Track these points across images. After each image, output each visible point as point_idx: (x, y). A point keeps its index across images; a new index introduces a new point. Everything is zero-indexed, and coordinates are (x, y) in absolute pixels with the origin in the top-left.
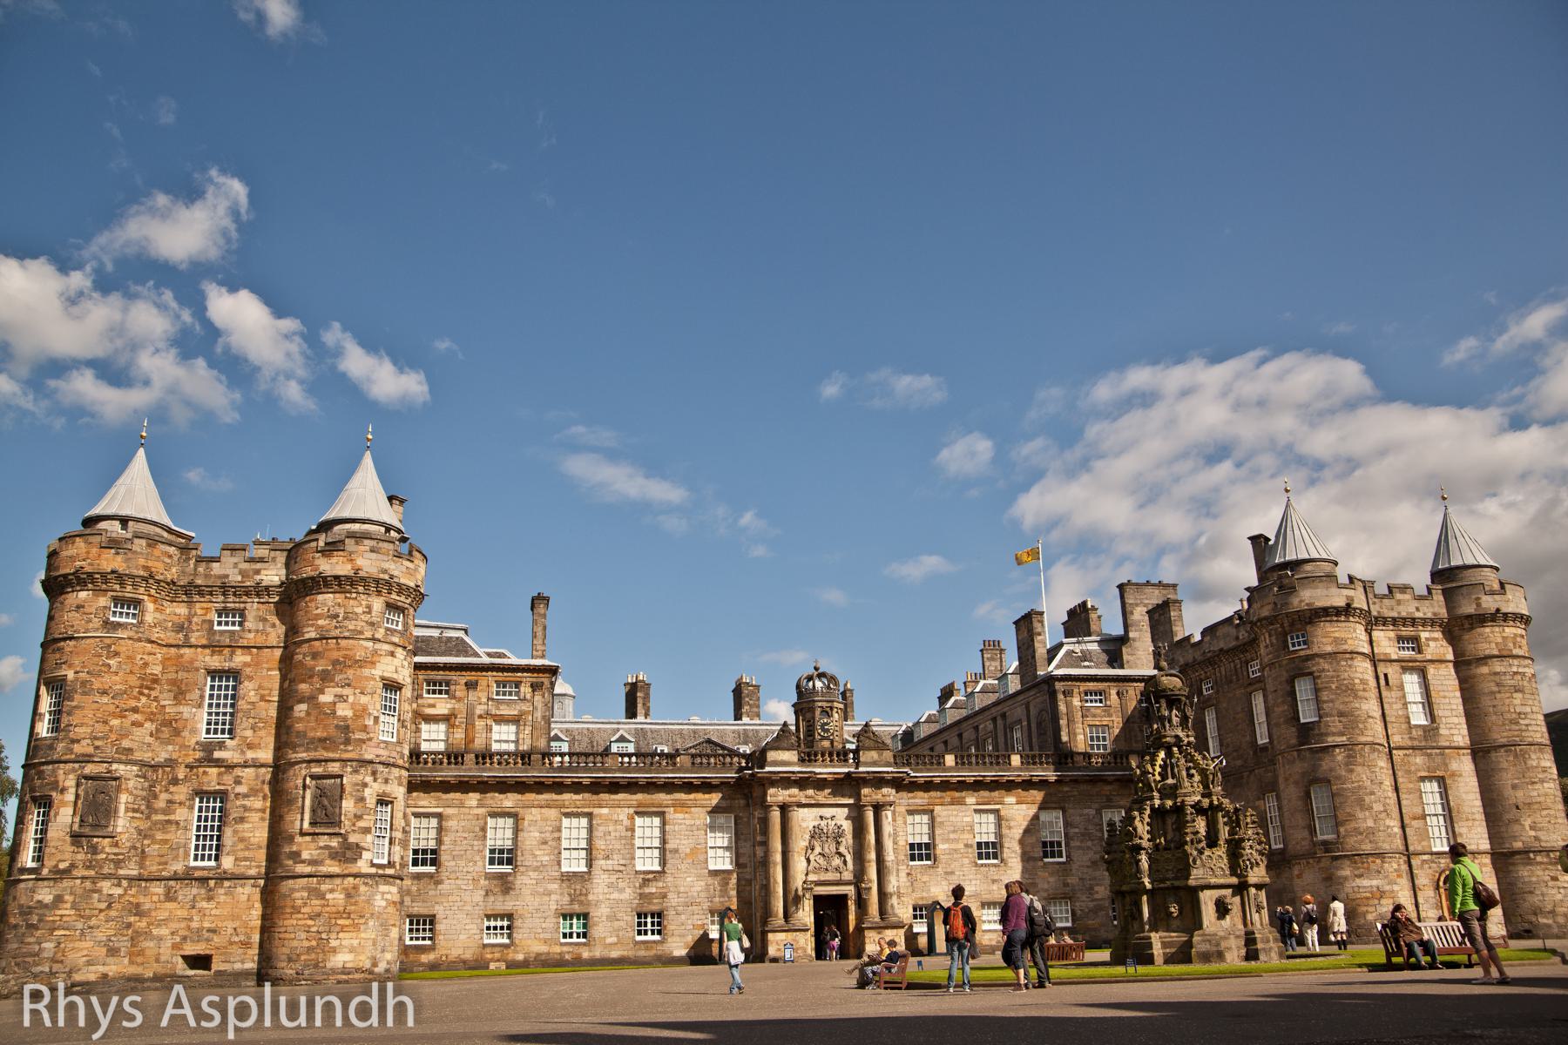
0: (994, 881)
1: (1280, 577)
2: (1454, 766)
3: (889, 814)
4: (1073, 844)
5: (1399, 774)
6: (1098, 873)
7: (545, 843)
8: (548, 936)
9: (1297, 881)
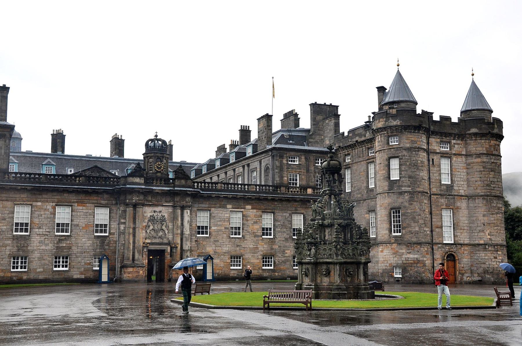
0: (238, 246)
1: (390, 108)
2: (458, 204)
3: (189, 211)
4: (277, 230)
5: (433, 206)
6: (288, 244)
7: (5, 219)
8: (4, 268)
9: (380, 254)
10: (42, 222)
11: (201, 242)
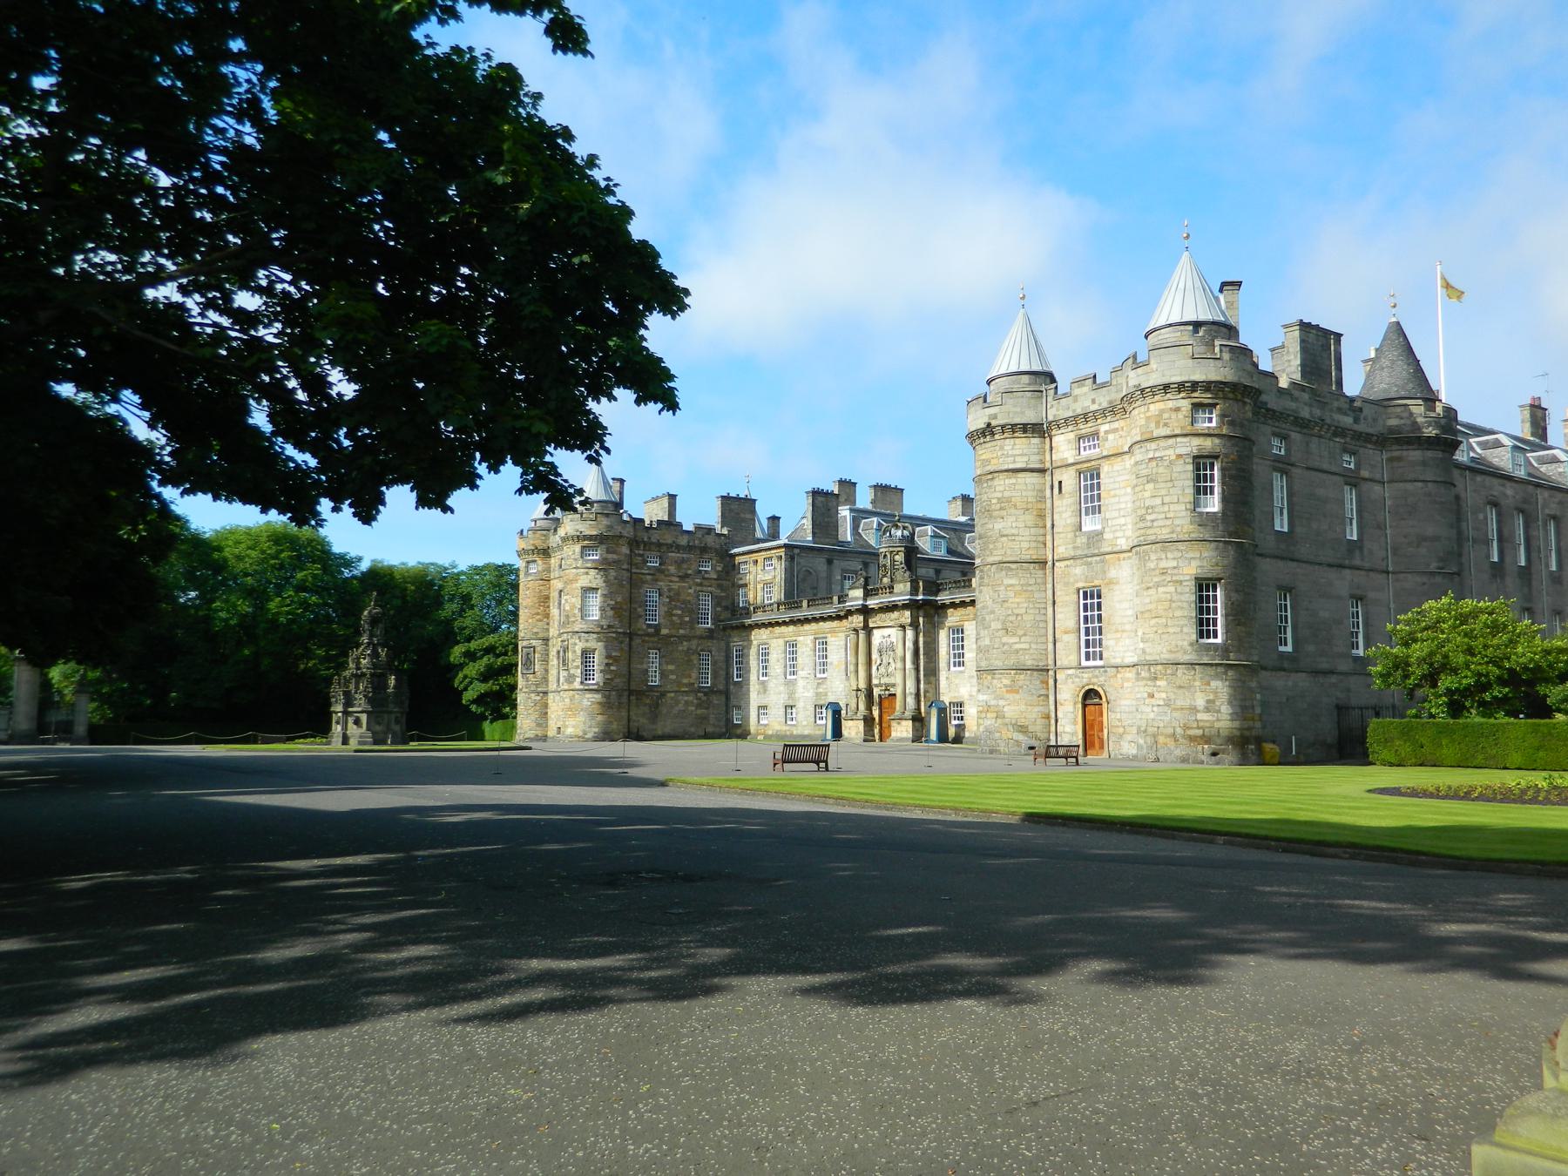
2: (1112, 573)
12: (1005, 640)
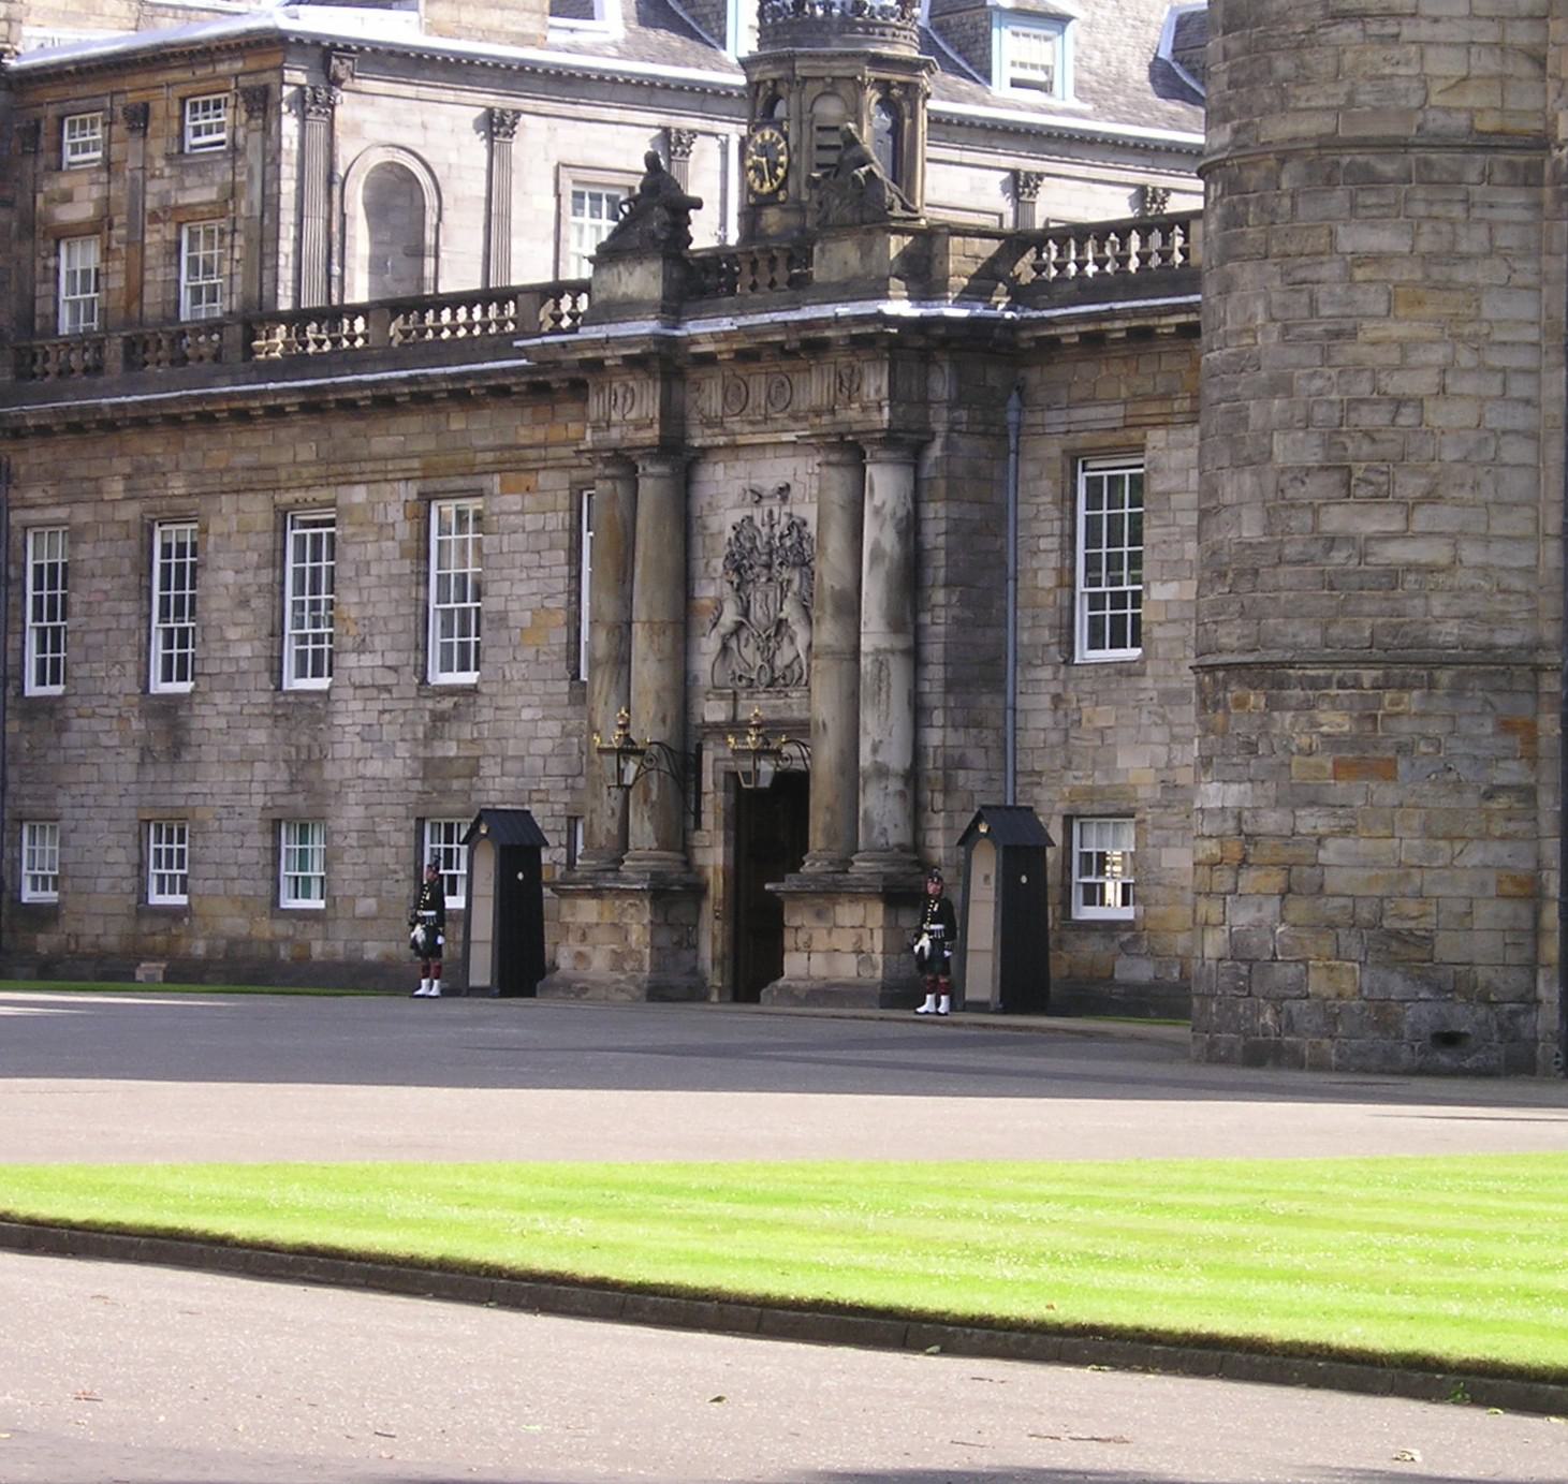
7: (244, 603)
10: (369, 611)
11: (1087, 710)
12: (1336, 519)
